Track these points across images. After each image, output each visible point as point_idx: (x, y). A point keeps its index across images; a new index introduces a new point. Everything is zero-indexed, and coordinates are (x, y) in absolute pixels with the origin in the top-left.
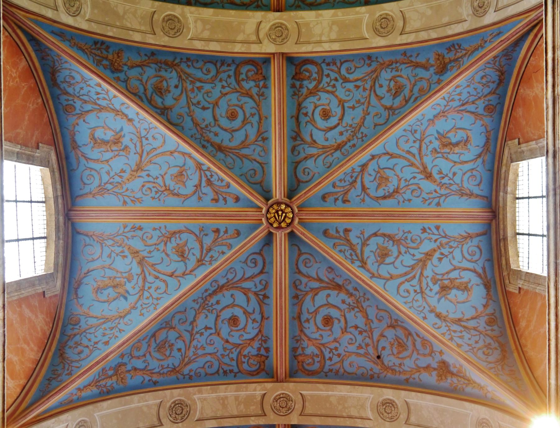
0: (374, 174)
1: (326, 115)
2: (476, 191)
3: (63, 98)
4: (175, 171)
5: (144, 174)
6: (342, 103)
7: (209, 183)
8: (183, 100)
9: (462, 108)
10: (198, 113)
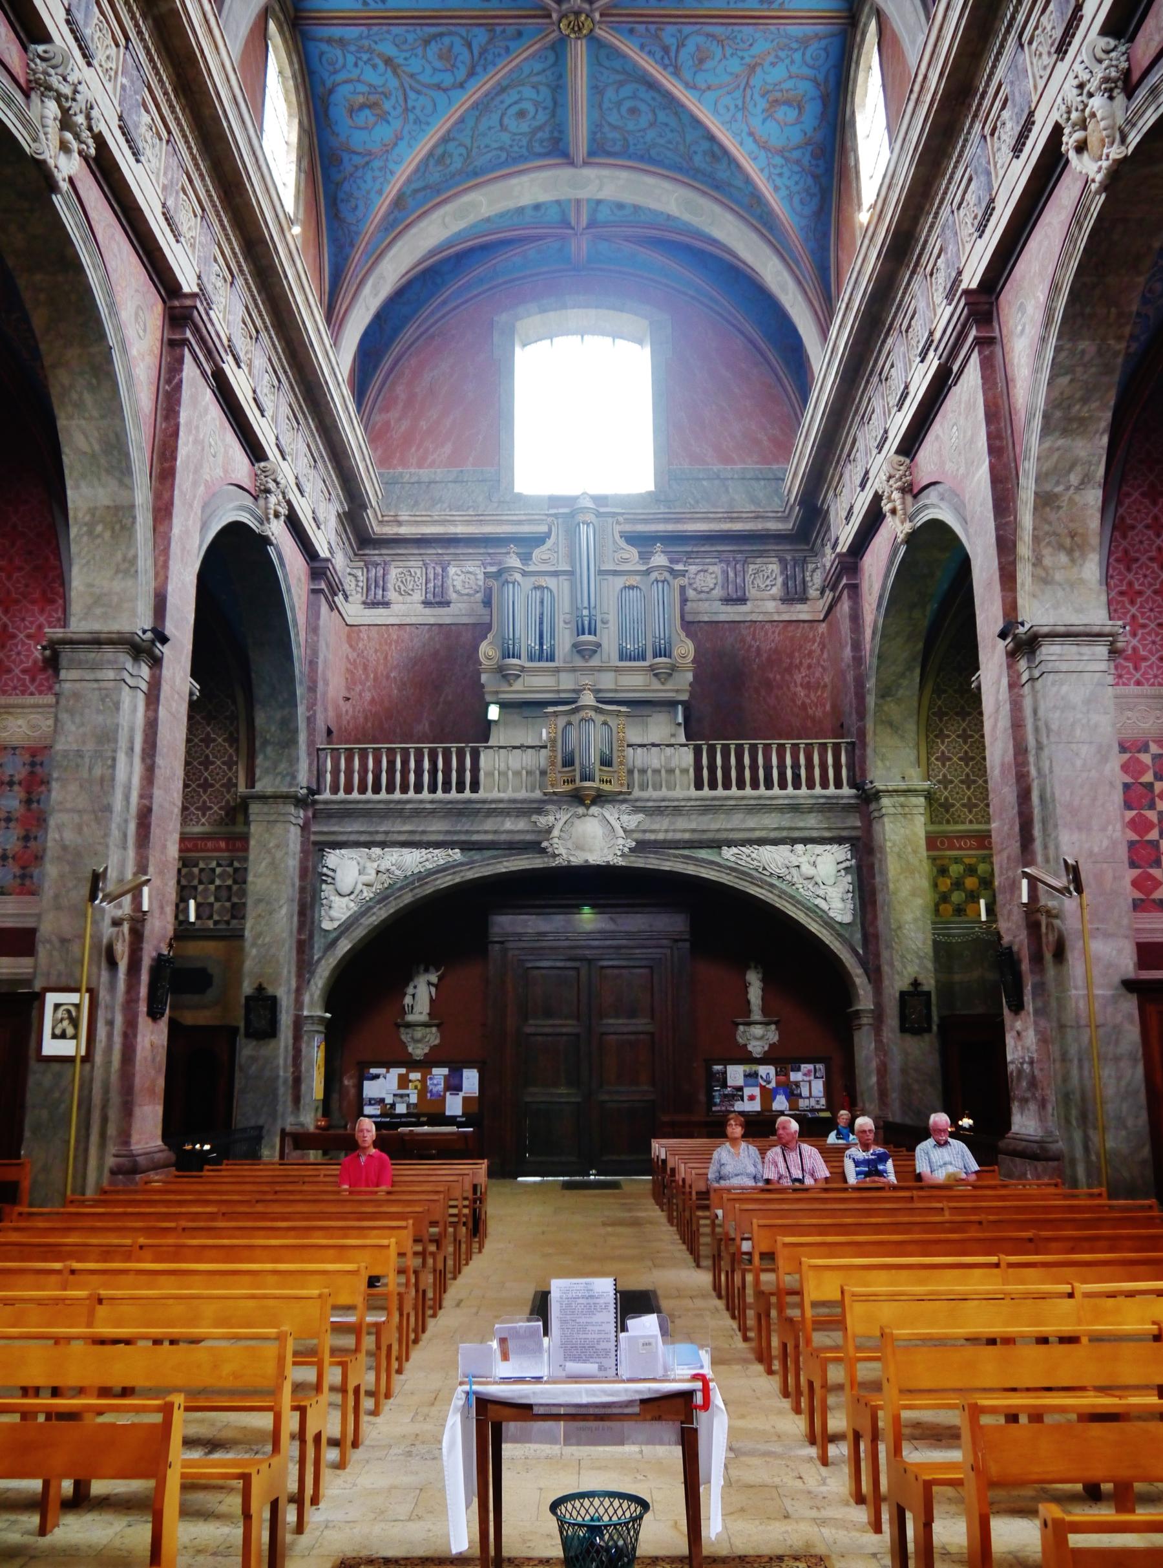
0: (459, 64)
1: (522, 114)
2: (324, 47)
3: (819, 171)
4: (708, 65)
5: (748, 60)
6: (503, 127)
7: (666, 50)
8: (689, 139)
9: (367, 159)
10: (673, 122)
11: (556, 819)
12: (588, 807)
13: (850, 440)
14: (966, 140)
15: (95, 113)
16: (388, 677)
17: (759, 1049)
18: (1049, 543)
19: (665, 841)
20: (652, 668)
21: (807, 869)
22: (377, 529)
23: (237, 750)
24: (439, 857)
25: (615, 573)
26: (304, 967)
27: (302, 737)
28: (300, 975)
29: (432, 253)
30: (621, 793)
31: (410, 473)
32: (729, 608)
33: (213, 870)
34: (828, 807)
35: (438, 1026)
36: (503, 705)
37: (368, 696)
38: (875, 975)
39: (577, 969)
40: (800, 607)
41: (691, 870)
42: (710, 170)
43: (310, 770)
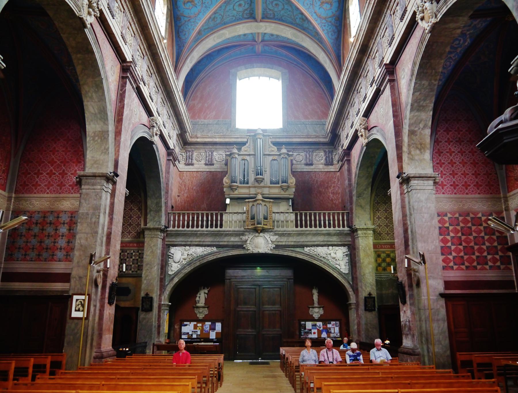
3: (338, 25)
6: (234, 10)
8: (295, 14)
10: (290, 9)
11: (248, 237)
12: (259, 233)
13: (347, 112)
14: (385, 16)
15: (100, 3)
16: (192, 189)
17: (317, 316)
18: (413, 147)
19: (285, 245)
20: (281, 187)
21: (333, 255)
22: (190, 140)
23: (141, 213)
24: (209, 250)
25: (269, 155)
26: (162, 287)
27: (163, 209)
28: (161, 290)
29: (210, 49)
30: (270, 229)
31: (202, 121)
32: (307, 167)
33: (132, 254)
34: (340, 234)
35: (207, 308)
36: (231, 199)
37: (186, 195)
38: (356, 291)
39: (255, 288)
40: (331, 167)
41: (294, 255)
42: (302, 24)
43: (166, 220)
